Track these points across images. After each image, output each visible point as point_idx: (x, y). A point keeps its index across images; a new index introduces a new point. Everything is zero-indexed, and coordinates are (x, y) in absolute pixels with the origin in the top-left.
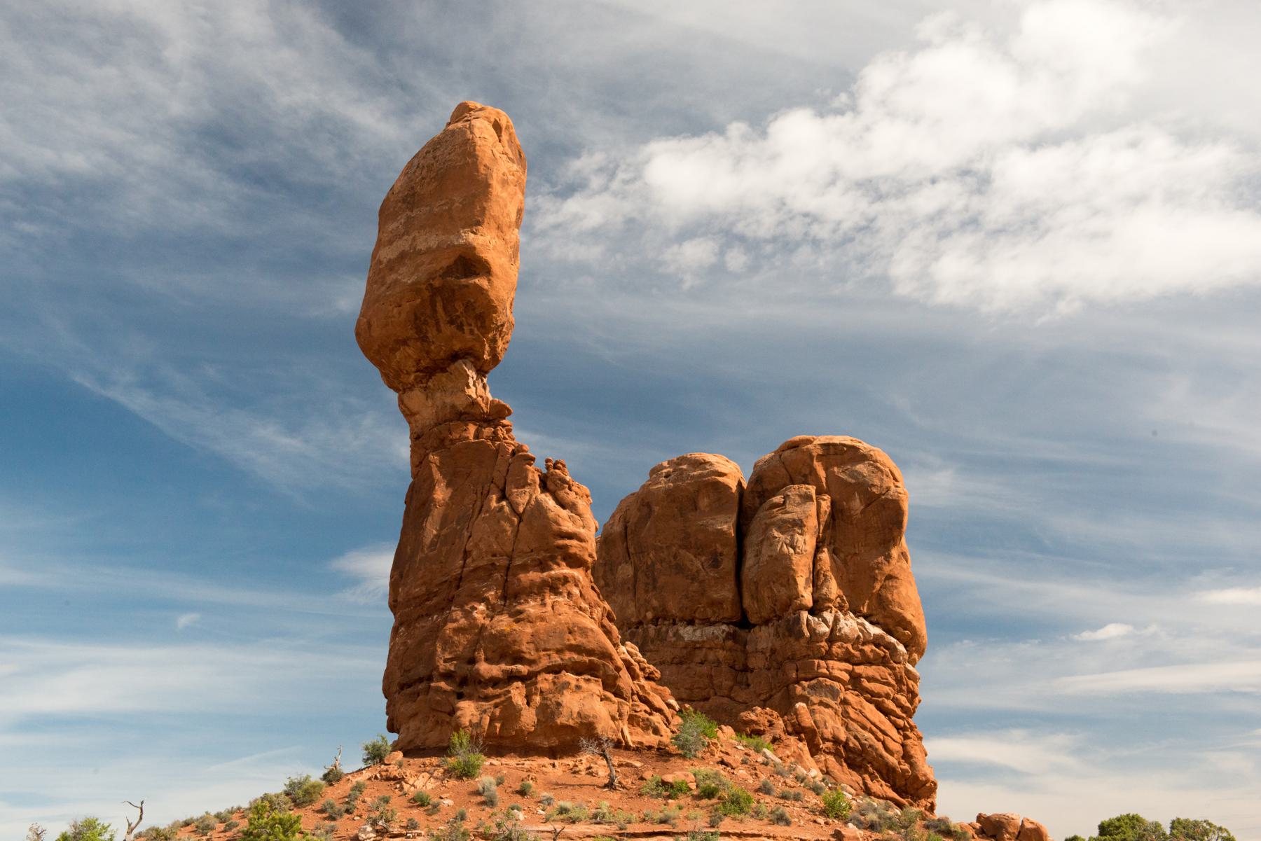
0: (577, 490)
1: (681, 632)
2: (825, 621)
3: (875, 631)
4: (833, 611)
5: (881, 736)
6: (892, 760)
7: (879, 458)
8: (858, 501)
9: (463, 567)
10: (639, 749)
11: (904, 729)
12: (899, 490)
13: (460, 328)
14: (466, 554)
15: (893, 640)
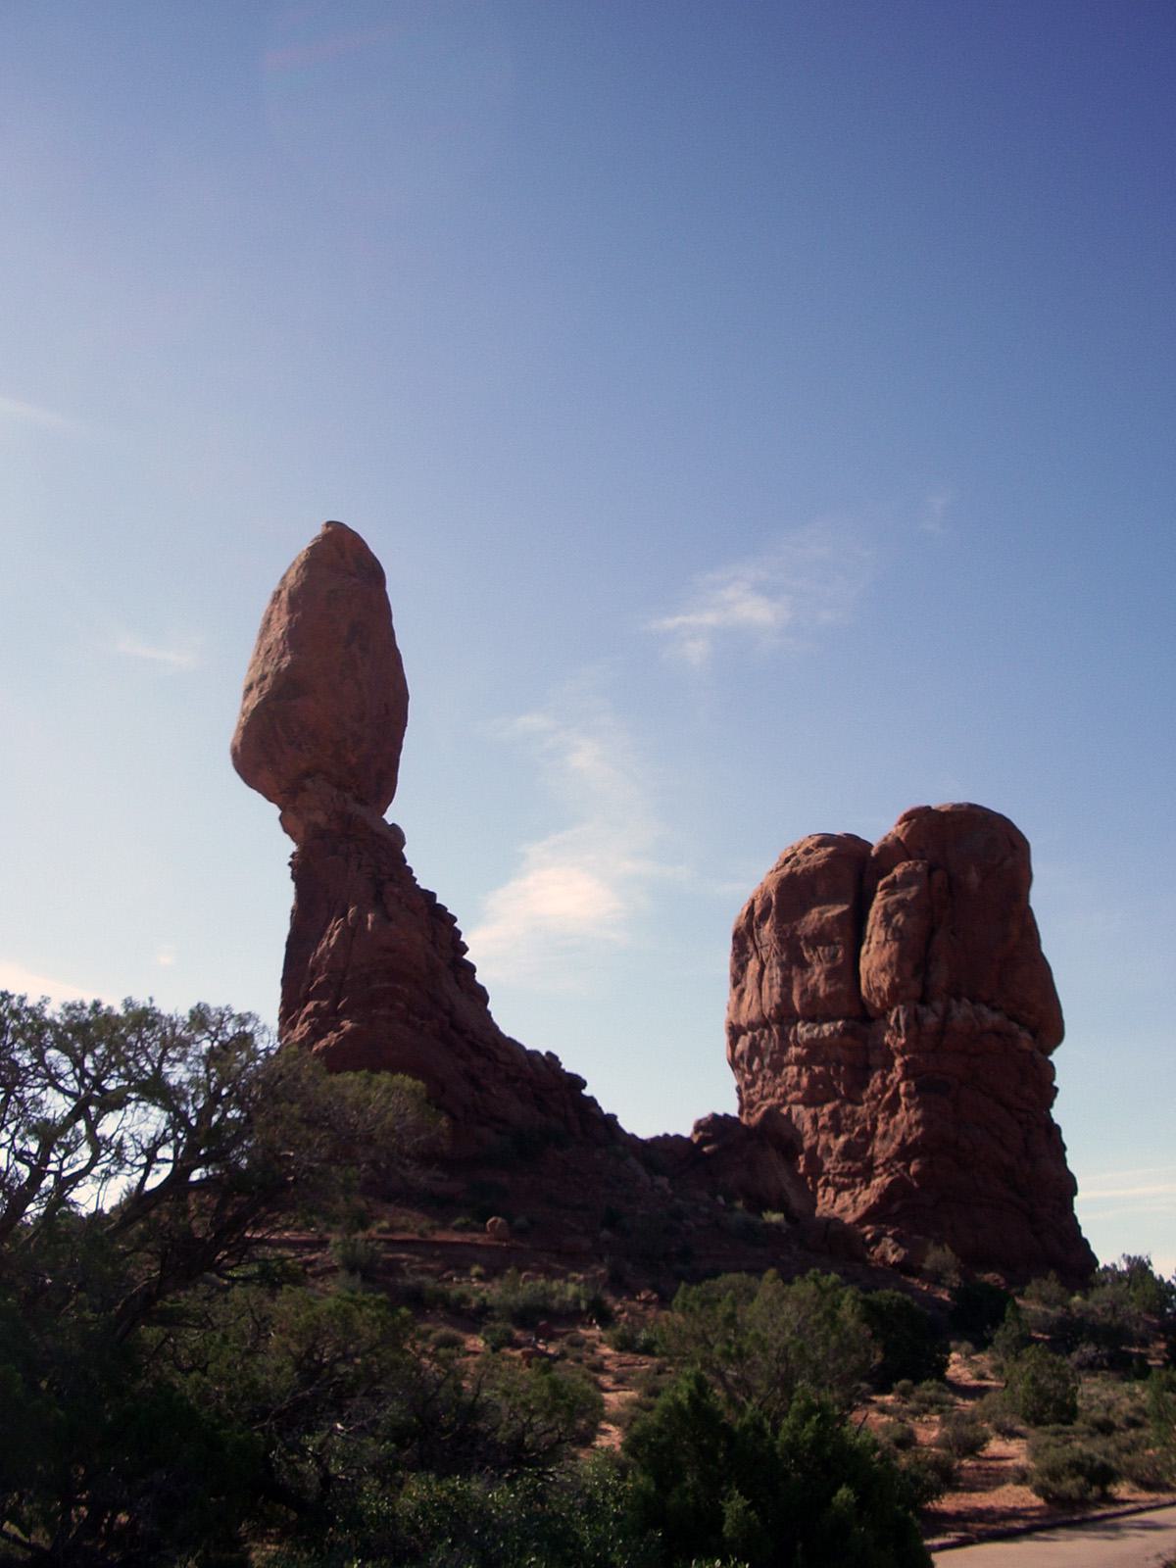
3: (993, 1019)
8: (974, 874)
15: (1015, 1026)
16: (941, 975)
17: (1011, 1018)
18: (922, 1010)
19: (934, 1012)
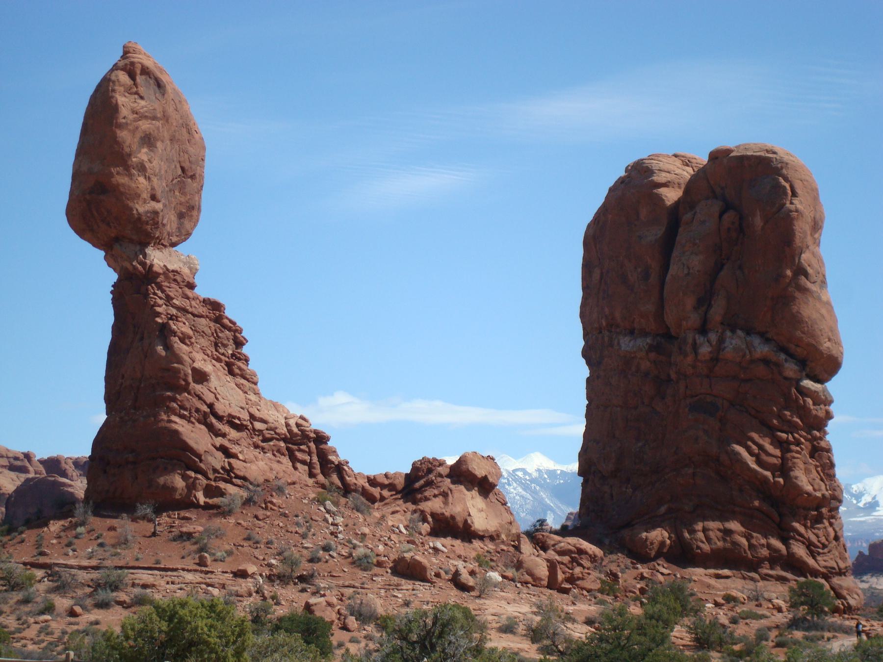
0: (181, 335)
1: (621, 341)
2: (708, 341)
3: (762, 349)
4: (720, 331)
5: (755, 448)
6: (768, 474)
7: (784, 171)
8: (759, 217)
9: (122, 384)
10: (207, 507)
11: (787, 442)
12: (792, 207)
13: (108, 224)
14: (123, 377)
15: (783, 356)
16: (717, 311)
17: (783, 349)
18: (700, 339)
19: (708, 341)
